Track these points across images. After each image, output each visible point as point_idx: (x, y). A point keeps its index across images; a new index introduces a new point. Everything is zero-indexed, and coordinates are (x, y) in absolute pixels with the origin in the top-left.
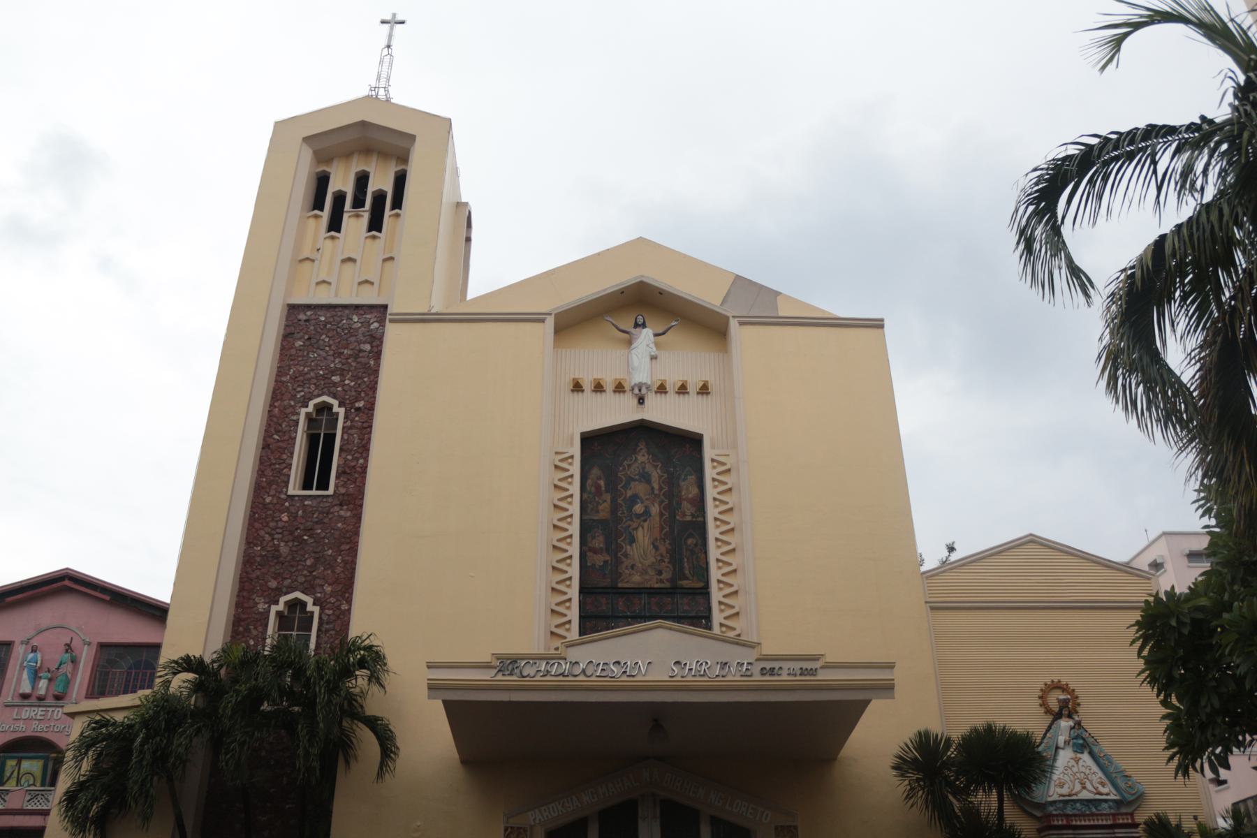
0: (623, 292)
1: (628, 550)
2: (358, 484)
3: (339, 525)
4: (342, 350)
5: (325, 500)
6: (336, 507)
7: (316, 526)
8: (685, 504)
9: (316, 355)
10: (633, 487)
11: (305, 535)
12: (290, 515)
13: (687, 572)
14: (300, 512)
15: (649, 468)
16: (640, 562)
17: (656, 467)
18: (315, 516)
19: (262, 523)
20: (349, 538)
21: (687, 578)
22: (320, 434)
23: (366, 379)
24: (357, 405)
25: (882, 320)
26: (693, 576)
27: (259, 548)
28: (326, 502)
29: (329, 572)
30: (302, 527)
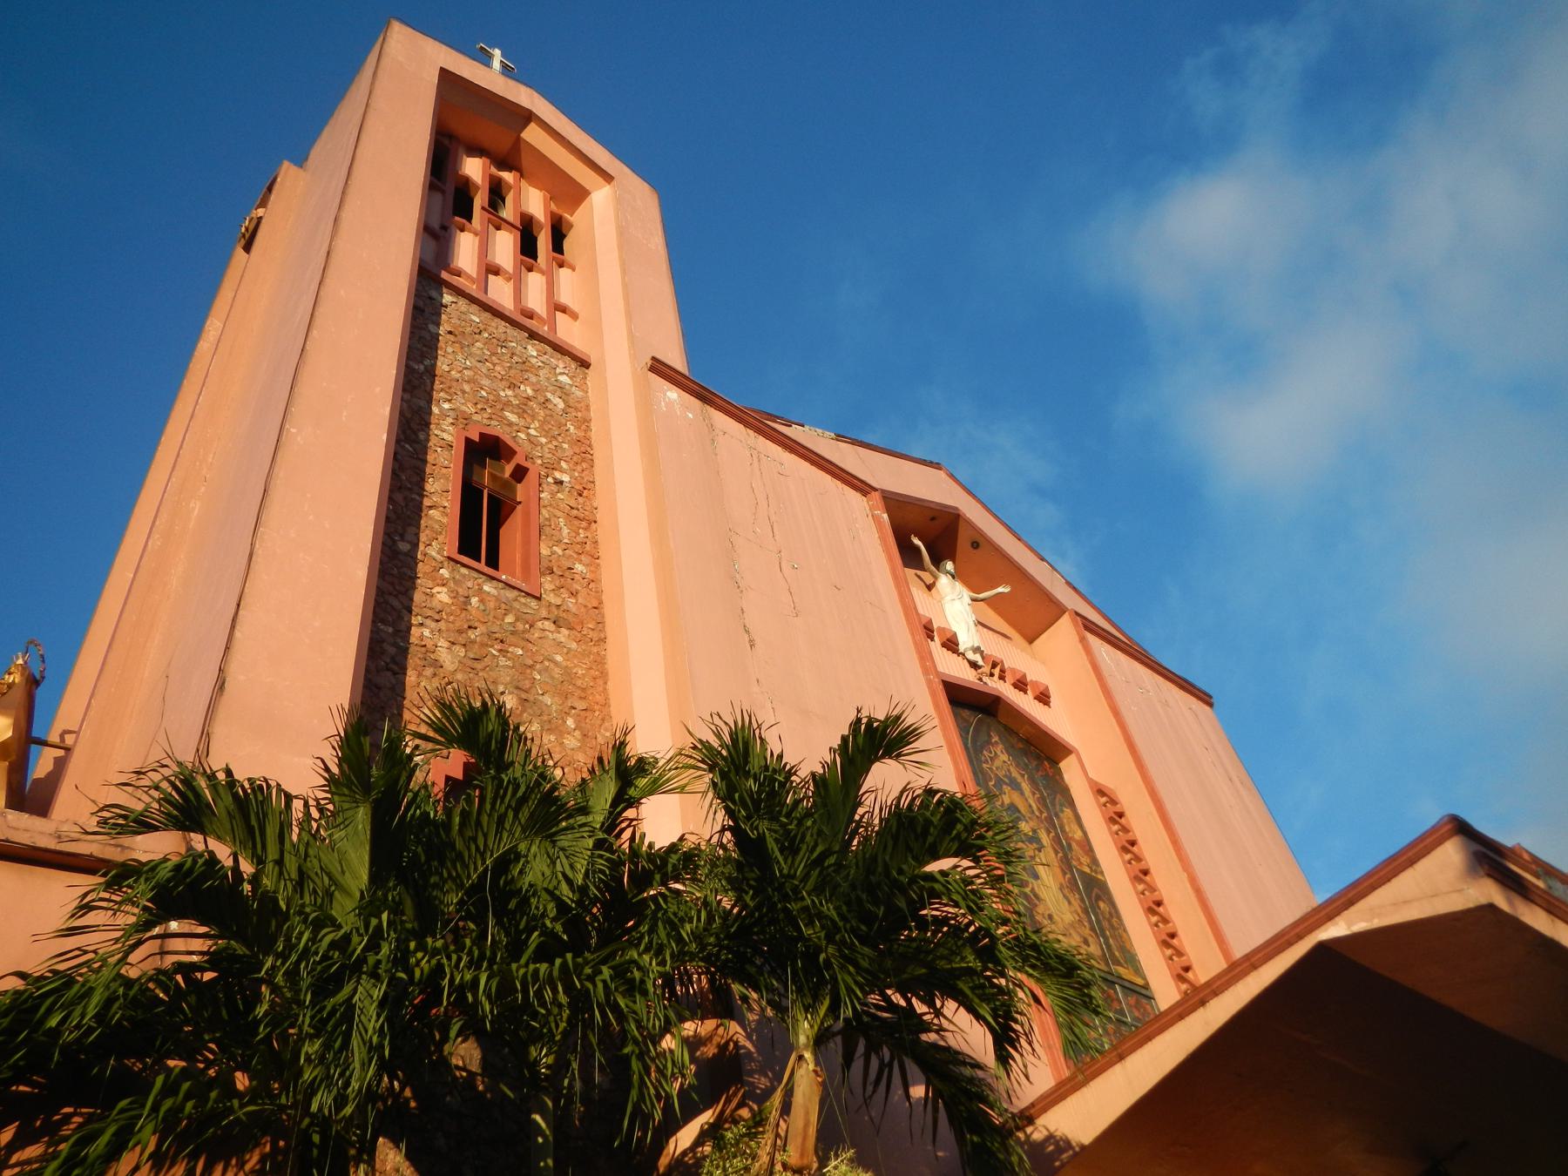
0: (933, 519)
1: (1036, 889)
2: (580, 600)
3: (559, 658)
4: (519, 384)
5: (523, 600)
6: (546, 623)
7: (512, 639)
8: (1074, 845)
9: (468, 363)
10: (1006, 791)
11: (492, 646)
12: (454, 595)
13: (1117, 953)
14: (474, 600)
15: (1015, 774)
16: (1057, 915)
17: (1023, 776)
18: (509, 619)
19: (392, 584)
20: (584, 690)
21: (1119, 964)
22: (482, 492)
23: (565, 446)
24: (558, 475)
25: (1211, 697)
26: (1126, 962)
27: (390, 630)
28: (525, 604)
29: (552, 738)
30: (481, 629)
